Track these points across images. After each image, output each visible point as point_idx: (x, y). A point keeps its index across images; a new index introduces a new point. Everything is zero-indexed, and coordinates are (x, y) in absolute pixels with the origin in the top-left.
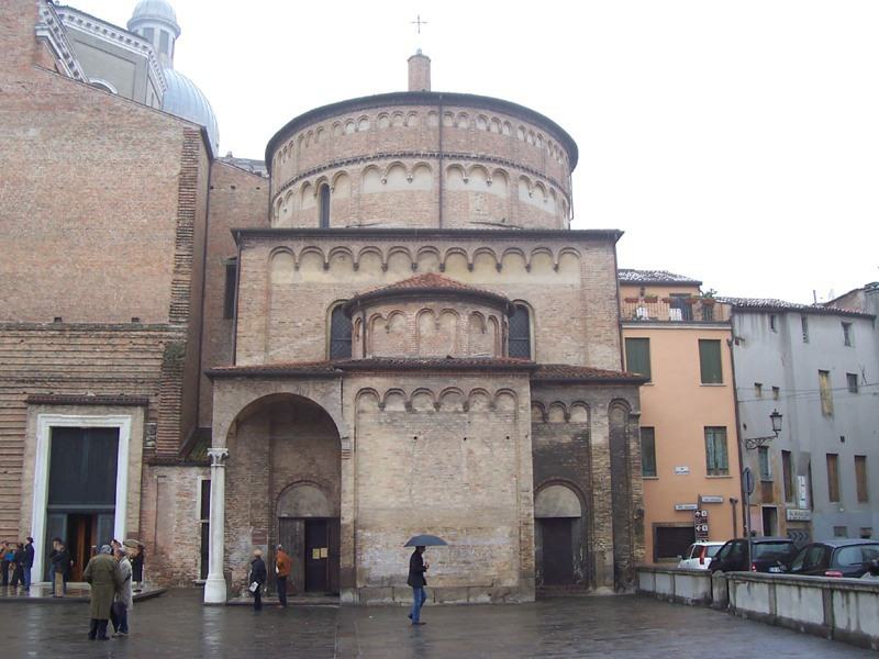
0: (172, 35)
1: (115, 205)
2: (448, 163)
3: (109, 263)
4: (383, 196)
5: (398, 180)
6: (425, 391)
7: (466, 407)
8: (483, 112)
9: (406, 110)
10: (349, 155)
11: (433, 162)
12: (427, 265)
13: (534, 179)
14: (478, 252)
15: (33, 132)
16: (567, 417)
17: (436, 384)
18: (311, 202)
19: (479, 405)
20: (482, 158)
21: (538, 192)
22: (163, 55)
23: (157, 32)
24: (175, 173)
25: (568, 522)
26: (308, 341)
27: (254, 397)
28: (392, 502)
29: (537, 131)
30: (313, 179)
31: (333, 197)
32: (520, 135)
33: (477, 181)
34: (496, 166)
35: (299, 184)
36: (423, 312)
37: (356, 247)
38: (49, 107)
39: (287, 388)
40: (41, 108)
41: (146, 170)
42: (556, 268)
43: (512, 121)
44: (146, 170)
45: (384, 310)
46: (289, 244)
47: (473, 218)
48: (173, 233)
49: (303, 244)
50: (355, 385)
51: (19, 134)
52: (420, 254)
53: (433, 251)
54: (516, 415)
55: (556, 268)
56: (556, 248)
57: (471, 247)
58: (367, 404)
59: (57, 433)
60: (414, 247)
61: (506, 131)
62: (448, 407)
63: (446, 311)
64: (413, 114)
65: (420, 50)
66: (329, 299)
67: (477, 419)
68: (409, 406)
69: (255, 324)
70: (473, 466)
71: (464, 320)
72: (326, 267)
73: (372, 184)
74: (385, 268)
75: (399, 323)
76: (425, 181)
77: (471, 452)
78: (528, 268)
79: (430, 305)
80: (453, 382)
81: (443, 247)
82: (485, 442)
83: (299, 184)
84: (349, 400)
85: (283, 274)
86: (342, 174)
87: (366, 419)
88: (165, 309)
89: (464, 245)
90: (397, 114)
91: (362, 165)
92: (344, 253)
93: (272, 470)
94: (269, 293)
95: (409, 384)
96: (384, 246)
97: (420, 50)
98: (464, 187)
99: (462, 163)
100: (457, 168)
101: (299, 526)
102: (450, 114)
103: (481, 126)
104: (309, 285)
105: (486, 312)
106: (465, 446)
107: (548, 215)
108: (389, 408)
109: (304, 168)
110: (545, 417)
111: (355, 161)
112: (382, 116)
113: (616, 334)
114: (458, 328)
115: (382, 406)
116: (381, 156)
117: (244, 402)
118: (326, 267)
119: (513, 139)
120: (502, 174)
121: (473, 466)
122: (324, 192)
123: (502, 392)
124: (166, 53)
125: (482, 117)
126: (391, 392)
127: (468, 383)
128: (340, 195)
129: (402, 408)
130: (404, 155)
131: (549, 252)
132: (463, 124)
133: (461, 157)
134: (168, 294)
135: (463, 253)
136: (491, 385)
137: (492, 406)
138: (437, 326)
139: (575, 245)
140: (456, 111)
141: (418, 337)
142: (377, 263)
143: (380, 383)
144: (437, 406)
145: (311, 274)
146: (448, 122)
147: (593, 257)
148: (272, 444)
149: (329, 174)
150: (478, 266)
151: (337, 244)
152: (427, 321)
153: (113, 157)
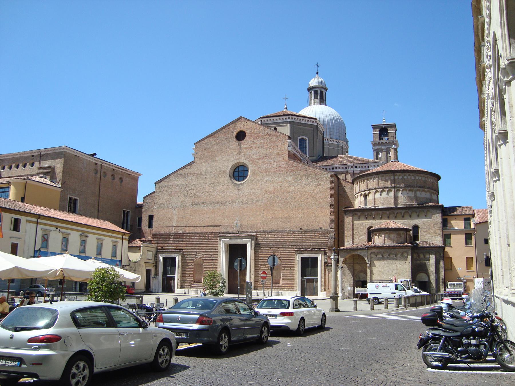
0: (324, 91)
1: (313, 197)
3: (313, 213)
8: (405, 174)
9: (385, 175)
10: (371, 187)
11: (393, 190)
13: (421, 189)
15: (290, 178)
16: (424, 256)
18: (363, 198)
19: (399, 256)
21: (423, 193)
22: (322, 100)
23: (319, 92)
25: (426, 282)
26: (362, 237)
29: (422, 175)
30: (363, 193)
32: (417, 178)
34: (409, 188)
35: (360, 194)
37: (373, 213)
38: (294, 170)
39: (356, 253)
40: (291, 171)
41: (321, 186)
42: (426, 216)
43: (414, 174)
44: (321, 186)
46: (357, 213)
47: (403, 203)
49: (360, 213)
50: (370, 251)
53: (393, 213)
55: (426, 216)
56: (425, 210)
57: (403, 212)
58: (373, 255)
59: (303, 259)
60: (388, 212)
61: (413, 178)
62: (391, 256)
63: (390, 234)
66: (367, 226)
68: (382, 255)
70: (397, 269)
71: (396, 235)
76: (392, 194)
81: (396, 212)
83: (360, 194)
84: (369, 255)
86: (370, 193)
87: (373, 259)
88: (328, 225)
89: (401, 211)
91: (375, 191)
93: (354, 270)
95: (382, 251)
96: (381, 212)
101: (360, 282)
102: (396, 175)
103: (405, 177)
105: (401, 232)
107: (427, 198)
108: (378, 256)
109: (361, 189)
110: (419, 256)
111: (373, 189)
113: (441, 233)
119: (415, 179)
121: (397, 269)
122: (366, 196)
124: (323, 99)
125: (405, 175)
126: (378, 253)
128: (370, 197)
129: (381, 256)
131: (424, 211)
132: (400, 178)
134: (329, 221)
135: (401, 213)
136: (401, 250)
140: (398, 174)
143: (376, 251)
144: (389, 255)
146: (396, 178)
148: (353, 264)
149: (367, 192)
150: (405, 216)
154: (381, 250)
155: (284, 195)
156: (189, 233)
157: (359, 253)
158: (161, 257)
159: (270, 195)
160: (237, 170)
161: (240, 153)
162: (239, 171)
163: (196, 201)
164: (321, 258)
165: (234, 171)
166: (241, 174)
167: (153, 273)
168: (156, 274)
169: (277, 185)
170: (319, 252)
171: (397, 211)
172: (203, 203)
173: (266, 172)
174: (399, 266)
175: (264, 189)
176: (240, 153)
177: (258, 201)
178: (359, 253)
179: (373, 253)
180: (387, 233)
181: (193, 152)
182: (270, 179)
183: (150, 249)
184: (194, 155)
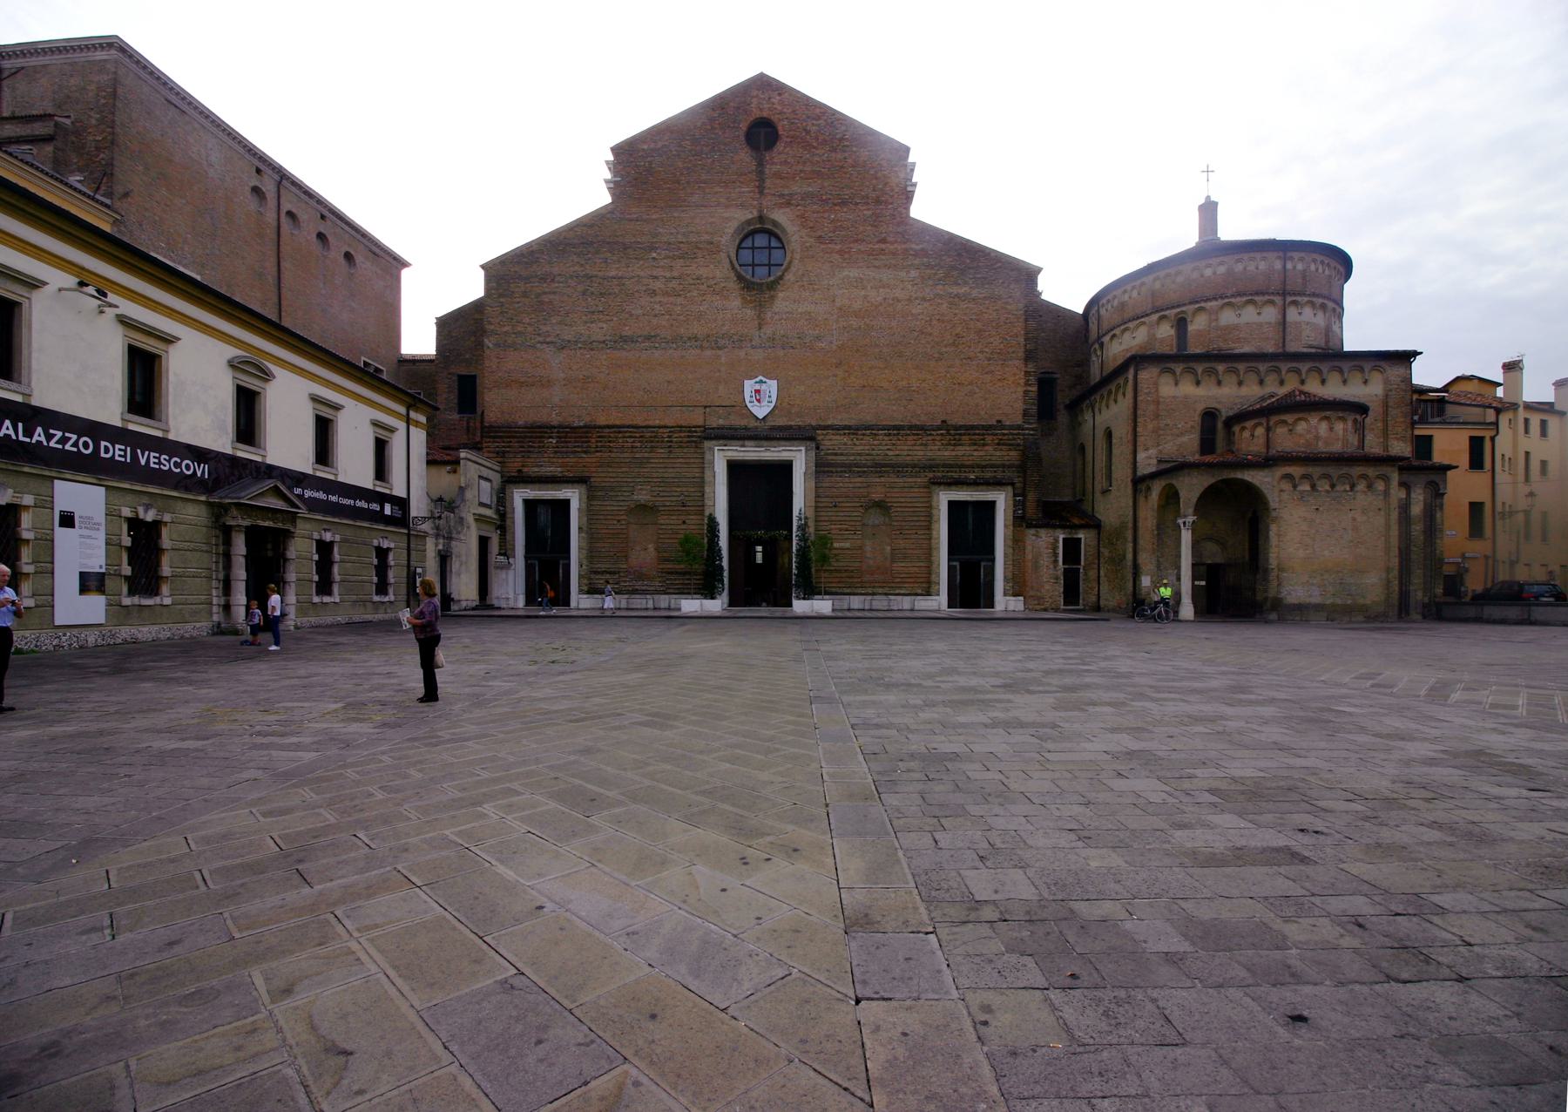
2: (1289, 299)
4: (1236, 327)
5: (1249, 315)
6: (1327, 476)
7: (1353, 487)
9: (1258, 255)
11: (1278, 300)
12: (1291, 385)
14: (1310, 370)
15: (914, 273)
17: (1333, 471)
19: (1361, 486)
20: (1314, 295)
24: (1021, 306)
26: (1185, 439)
27: (1212, 481)
28: (1301, 553)
31: (1191, 328)
33: (1308, 311)
34: (1321, 300)
36: (1322, 419)
37: (1221, 368)
45: (1289, 418)
46: (1172, 366)
48: (1021, 354)
51: (903, 274)
52: (1268, 371)
53: (1277, 370)
54: (1386, 493)
58: (1286, 486)
64: (1264, 259)
65: (1208, 197)
66: (1200, 407)
67: (1360, 497)
68: (1313, 487)
69: (1150, 426)
70: (1355, 529)
71: (1350, 423)
72: (1198, 383)
73: (1228, 317)
74: (1240, 383)
75: (1301, 427)
76: (1270, 314)
77: (1354, 519)
78: (1345, 382)
79: (1328, 413)
80: (1345, 470)
82: (1364, 511)
85: (1167, 389)
86: (1201, 309)
87: (1285, 496)
90: (1252, 259)
91: (1220, 302)
92: (1211, 372)
94: (1158, 403)
95: (1315, 471)
96: (1241, 367)
97: (1208, 197)
98: (1298, 318)
99: (1299, 299)
100: (1294, 303)
102: (1291, 258)
104: (1186, 397)
106: (1351, 515)
108: (1300, 488)
111: (1215, 299)
112: (1238, 261)
114: (1345, 430)
115: (1295, 487)
116: (1239, 294)
117: (1206, 484)
118: (1198, 383)
120: (1323, 307)
121: (1355, 529)
123: (1378, 477)
125: (1314, 261)
126: (1304, 477)
127: (1357, 471)
128: (1197, 324)
129: (1308, 488)
130: (1257, 294)
133: (1299, 294)
137: (1370, 486)
138: (1331, 429)
139: (1382, 363)
140: (1296, 255)
141: (1317, 438)
142: (1234, 379)
143: (1296, 471)
144: (1333, 486)
145: (1187, 388)
147: (1394, 372)
151: (1207, 365)
152: (1324, 426)
153: (975, 293)
154: (1310, 470)
155: (894, 324)
156: (608, 427)
157: (1250, 476)
158: (519, 496)
159: (854, 322)
160: (748, 243)
161: (761, 190)
162: (753, 248)
163: (627, 331)
164: (1002, 500)
165: (739, 247)
166: (761, 257)
167: (494, 547)
168: (506, 551)
169: (873, 293)
170: (997, 484)
171: (1290, 365)
172: (648, 338)
173: (841, 252)
174: (1359, 519)
175: (838, 303)
176: (761, 190)
177: (818, 338)
178: (1250, 476)
179: (1288, 477)
180: (1327, 418)
181: (609, 176)
182: (854, 273)
183: (485, 472)
184: (616, 188)
